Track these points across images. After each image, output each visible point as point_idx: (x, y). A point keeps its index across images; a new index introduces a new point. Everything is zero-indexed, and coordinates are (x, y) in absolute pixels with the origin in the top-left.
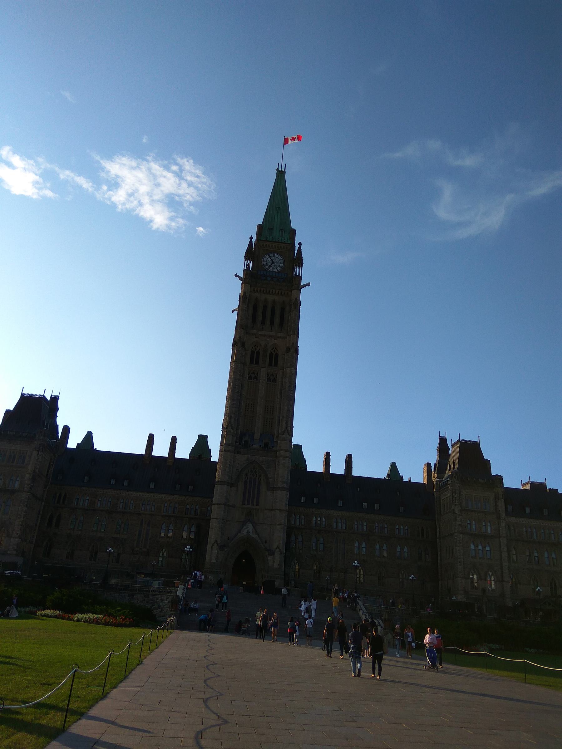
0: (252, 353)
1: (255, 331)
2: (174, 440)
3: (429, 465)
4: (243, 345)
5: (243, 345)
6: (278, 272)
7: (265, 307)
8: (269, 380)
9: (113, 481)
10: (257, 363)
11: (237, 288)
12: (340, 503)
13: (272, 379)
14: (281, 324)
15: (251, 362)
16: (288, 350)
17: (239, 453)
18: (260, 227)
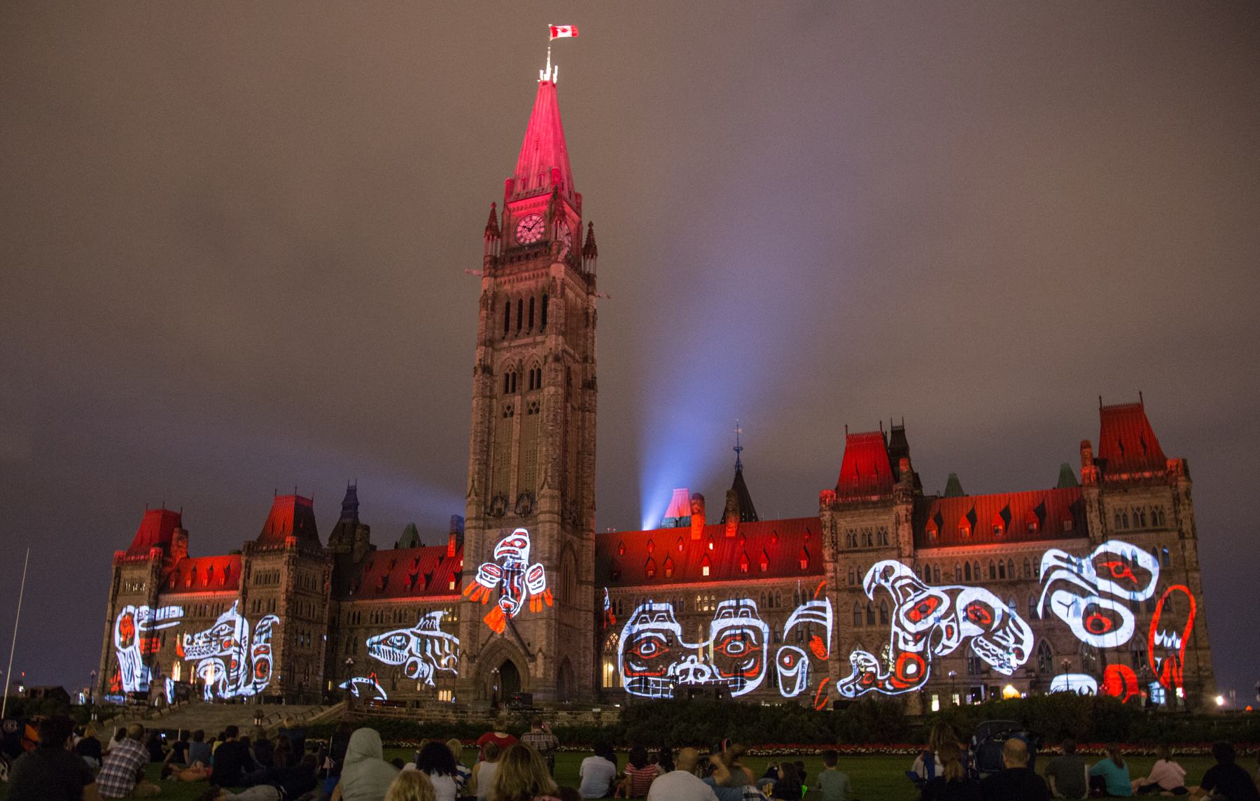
1: (506, 344)
7: (521, 302)
12: (706, 571)
17: (490, 528)
18: (511, 184)
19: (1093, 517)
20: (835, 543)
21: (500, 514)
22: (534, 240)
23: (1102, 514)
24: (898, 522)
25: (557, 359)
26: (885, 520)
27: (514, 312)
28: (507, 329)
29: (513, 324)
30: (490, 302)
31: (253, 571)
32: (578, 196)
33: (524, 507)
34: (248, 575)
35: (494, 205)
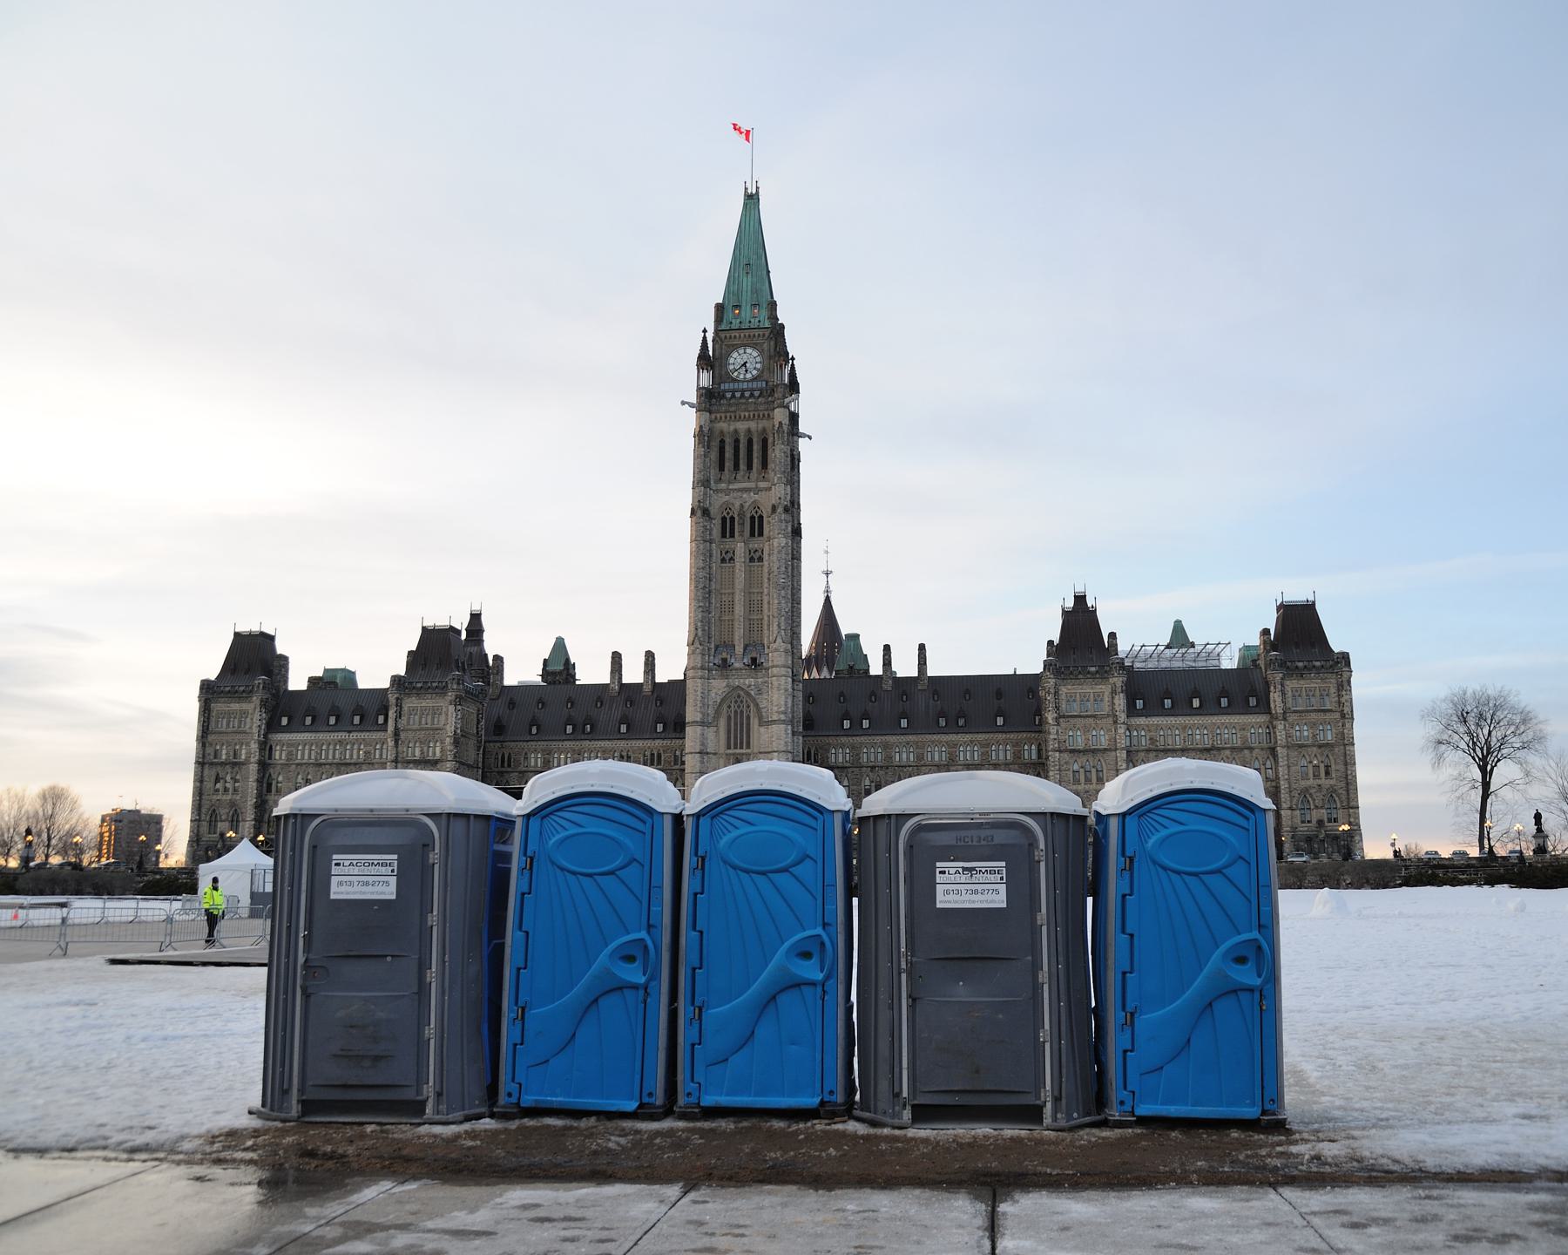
0: (724, 519)
2: (650, 658)
3: (1050, 643)
4: (706, 512)
5: (706, 512)
6: (755, 379)
7: (737, 441)
8: (752, 560)
9: (569, 729)
10: (732, 535)
11: (690, 420)
13: (755, 558)
14: (765, 464)
15: (724, 535)
16: (774, 508)
18: (720, 309)
19: (1275, 697)
20: (1057, 708)
21: (725, 665)
22: (749, 376)
23: (1283, 693)
24: (1114, 692)
25: (786, 510)
26: (1105, 689)
27: (729, 453)
28: (722, 468)
29: (729, 464)
30: (704, 437)
31: (405, 708)
32: (782, 326)
33: (754, 660)
34: (399, 715)
35: (705, 331)
